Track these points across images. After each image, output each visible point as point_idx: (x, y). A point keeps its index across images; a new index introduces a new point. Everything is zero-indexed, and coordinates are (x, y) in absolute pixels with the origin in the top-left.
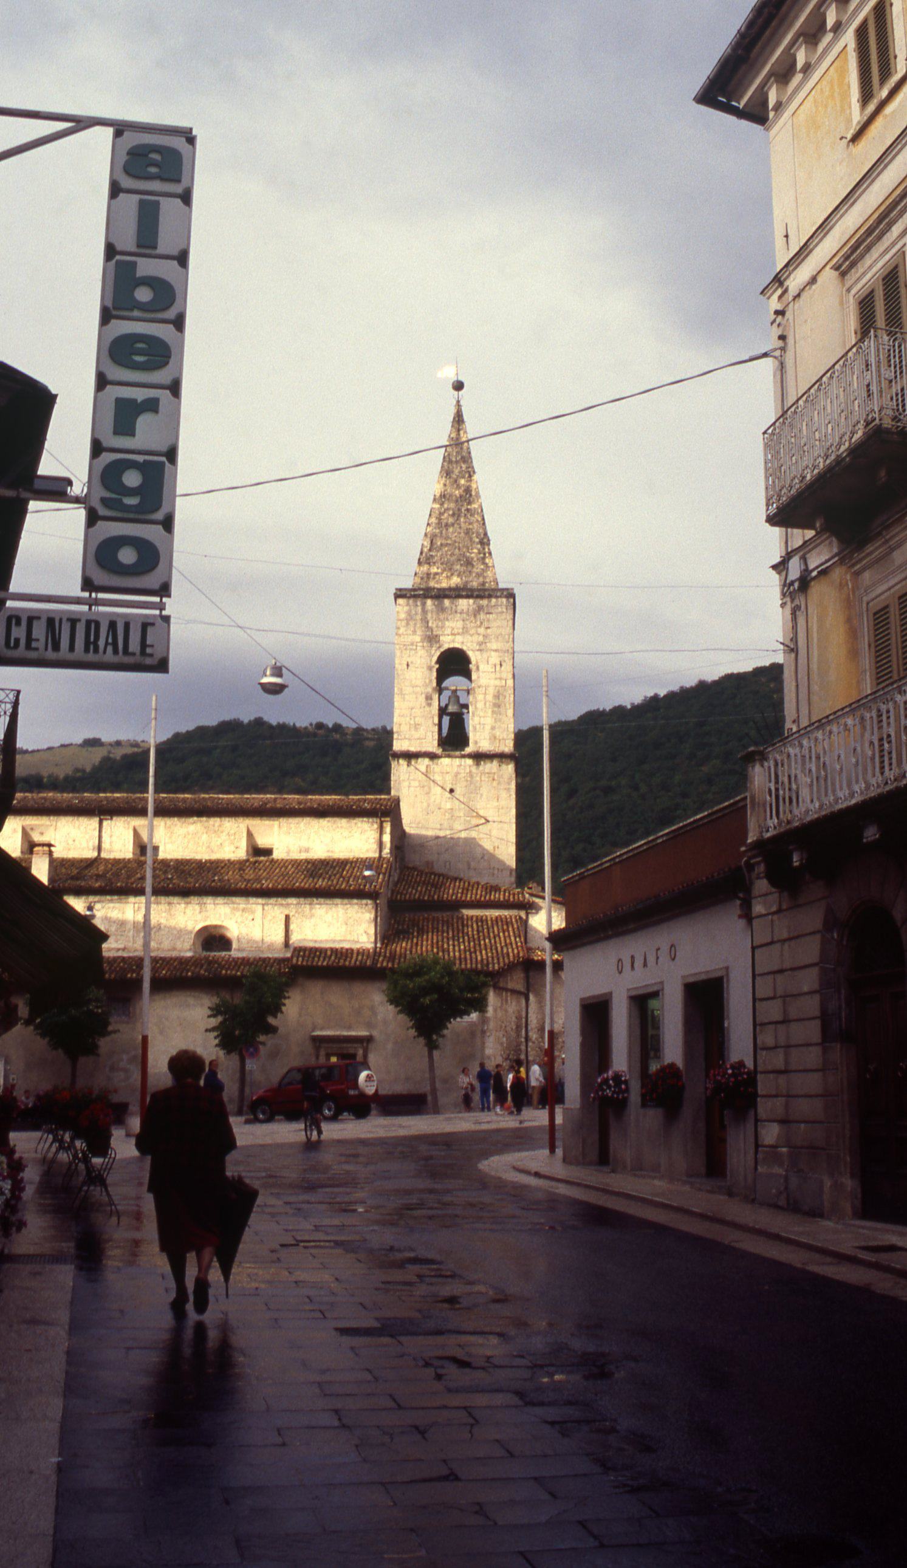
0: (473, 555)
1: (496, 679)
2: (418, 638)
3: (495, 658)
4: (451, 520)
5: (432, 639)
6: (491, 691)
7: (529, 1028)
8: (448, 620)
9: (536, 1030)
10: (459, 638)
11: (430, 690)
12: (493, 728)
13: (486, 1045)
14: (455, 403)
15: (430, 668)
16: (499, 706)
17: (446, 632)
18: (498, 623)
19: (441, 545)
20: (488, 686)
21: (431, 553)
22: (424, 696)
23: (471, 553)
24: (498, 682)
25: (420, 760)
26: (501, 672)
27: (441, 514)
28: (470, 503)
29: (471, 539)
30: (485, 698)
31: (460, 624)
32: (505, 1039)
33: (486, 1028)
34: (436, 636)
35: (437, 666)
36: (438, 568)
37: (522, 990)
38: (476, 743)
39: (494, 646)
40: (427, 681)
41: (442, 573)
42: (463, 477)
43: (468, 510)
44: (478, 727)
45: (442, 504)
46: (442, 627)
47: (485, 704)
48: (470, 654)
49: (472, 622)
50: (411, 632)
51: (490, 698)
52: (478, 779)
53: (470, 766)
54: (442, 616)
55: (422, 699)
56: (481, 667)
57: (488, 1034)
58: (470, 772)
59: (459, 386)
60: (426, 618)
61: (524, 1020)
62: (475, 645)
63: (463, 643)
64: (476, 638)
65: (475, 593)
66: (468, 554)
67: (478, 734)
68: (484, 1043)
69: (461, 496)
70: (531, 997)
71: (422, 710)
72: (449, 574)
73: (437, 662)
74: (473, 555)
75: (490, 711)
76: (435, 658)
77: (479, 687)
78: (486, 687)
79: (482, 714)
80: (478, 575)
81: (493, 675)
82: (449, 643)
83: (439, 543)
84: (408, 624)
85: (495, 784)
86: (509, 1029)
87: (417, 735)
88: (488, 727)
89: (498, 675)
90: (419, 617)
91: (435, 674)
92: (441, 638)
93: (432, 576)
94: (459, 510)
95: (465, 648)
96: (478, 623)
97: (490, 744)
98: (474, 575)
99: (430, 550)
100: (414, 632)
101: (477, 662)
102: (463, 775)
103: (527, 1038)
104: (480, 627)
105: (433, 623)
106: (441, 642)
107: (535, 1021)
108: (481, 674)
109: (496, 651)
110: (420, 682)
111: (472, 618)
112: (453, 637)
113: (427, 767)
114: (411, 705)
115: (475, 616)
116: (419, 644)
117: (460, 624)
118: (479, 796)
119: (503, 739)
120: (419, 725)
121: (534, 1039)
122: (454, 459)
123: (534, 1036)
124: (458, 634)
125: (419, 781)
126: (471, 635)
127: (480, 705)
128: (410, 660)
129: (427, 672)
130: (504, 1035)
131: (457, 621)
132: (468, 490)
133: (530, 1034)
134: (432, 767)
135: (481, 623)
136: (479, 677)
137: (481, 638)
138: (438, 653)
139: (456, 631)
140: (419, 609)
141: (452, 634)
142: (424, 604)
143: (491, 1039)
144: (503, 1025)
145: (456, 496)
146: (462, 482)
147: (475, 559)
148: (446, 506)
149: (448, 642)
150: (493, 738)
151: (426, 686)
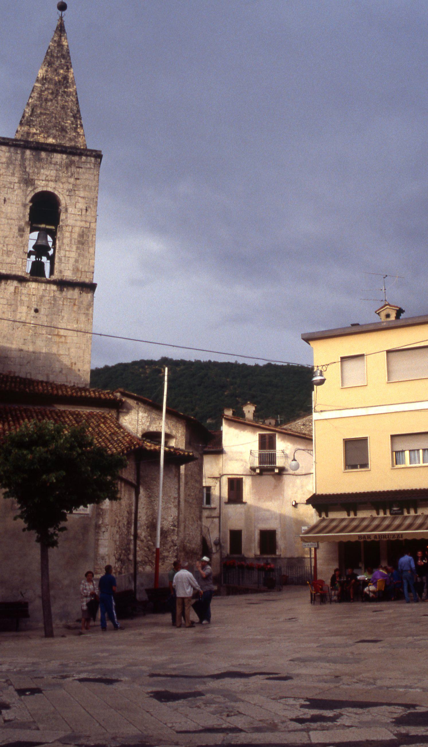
0: (67, 124)
1: (82, 221)
2: (17, 180)
3: (81, 205)
4: (50, 97)
5: (28, 182)
6: (77, 230)
7: (138, 525)
8: (43, 168)
9: (145, 527)
10: (52, 184)
11: (23, 223)
12: (77, 261)
13: (100, 542)
14: (58, 18)
15: (25, 205)
16: (83, 244)
17: (40, 178)
18: (87, 176)
19: (41, 113)
20: (74, 226)
21: (32, 118)
22: (17, 227)
23: (66, 123)
24: (83, 224)
25: (9, 282)
26: (86, 216)
27: (42, 91)
28: (66, 87)
29: (66, 113)
30: (71, 236)
31: (53, 173)
32: (118, 536)
33: (100, 522)
34: (32, 180)
35: (31, 204)
36: (36, 130)
37: (134, 482)
38: (61, 272)
39: (82, 194)
40: (21, 215)
41: (40, 134)
42: (62, 68)
43: (65, 92)
44: (63, 258)
45: (43, 84)
46: (38, 173)
47: (71, 240)
48: (61, 197)
49: (64, 172)
50: (10, 174)
51: (75, 236)
52: (61, 303)
53: (54, 291)
54: (38, 165)
55: (15, 230)
56: (70, 210)
57: (103, 529)
58: (54, 296)
59: (62, 7)
60: (24, 164)
61: (133, 515)
62: (65, 191)
63: (55, 188)
64: (66, 186)
65: (69, 150)
66: (63, 123)
67: (63, 265)
68: (98, 540)
69: (59, 81)
70: (142, 491)
71: (14, 240)
72: (46, 136)
73: (32, 201)
74: (67, 124)
75: (74, 248)
76: (29, 198)
77: (67, 226)
78: (73, 227)
79: (67, 249)
80: (71, 140)
81: (78, 218)
82: (43, 187)
83: (39, 112)
84: (8, 167)
85: (75, 308)
86: (121, 524)
87: (8, 260)
88: (72, 261)
89: (84, 218)
90: (18, 163)
91: (28, 211)
92: (36, 182)
93: (31, 135)
94: (57, 90)
95: (56, 193)
96: (69, 174)
97: (73, 274)
98: (67, 139)
99: (31, 116)
100: (13, 174)
101: (66, 205)
102: (47, 298)
103: (136, 536)
104: (71, 177)
105: (30, 169)
106: (36, 186)
107: (144, 518)
108: (69, 215)
109: (83, 198)
110: (14, 216)
111: (65, 169)
112: (47, 182)
113: (15, 288)
114: (6, 233)
115: (67, 168)
116: (16, 185)
117: (53, 173)
118: (61, 317)
119: (85, 271)
120: (10, 251)
121: (142, 537)
122: (55, 55)
123: (143, 534)
124: (52, 181)
125: (7, 300)
126: (63, 183)
127: (66, 241)
128: (7, 196)
129: (22, 208)
130: (117, 532)
131: (51, 170)
132: (66, 78)
133: (139, 531)
134: (20, 288)
135: (72, 174)
136: (66, 218)
137: (71, 187)
138: (33, 194)
139: (49, 178)
140: (19, 156)
141: (46, 180)
142: (23, 153)
143: (107, 535)
144: (118, 520)
145: (55, 80)
146: (61, 71)
147: (69, 128)
148: (46, 86)
149: (42, 186)
150: (76, 270)
151: (19, 219)
